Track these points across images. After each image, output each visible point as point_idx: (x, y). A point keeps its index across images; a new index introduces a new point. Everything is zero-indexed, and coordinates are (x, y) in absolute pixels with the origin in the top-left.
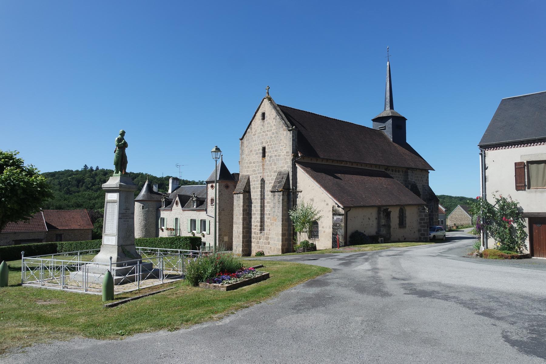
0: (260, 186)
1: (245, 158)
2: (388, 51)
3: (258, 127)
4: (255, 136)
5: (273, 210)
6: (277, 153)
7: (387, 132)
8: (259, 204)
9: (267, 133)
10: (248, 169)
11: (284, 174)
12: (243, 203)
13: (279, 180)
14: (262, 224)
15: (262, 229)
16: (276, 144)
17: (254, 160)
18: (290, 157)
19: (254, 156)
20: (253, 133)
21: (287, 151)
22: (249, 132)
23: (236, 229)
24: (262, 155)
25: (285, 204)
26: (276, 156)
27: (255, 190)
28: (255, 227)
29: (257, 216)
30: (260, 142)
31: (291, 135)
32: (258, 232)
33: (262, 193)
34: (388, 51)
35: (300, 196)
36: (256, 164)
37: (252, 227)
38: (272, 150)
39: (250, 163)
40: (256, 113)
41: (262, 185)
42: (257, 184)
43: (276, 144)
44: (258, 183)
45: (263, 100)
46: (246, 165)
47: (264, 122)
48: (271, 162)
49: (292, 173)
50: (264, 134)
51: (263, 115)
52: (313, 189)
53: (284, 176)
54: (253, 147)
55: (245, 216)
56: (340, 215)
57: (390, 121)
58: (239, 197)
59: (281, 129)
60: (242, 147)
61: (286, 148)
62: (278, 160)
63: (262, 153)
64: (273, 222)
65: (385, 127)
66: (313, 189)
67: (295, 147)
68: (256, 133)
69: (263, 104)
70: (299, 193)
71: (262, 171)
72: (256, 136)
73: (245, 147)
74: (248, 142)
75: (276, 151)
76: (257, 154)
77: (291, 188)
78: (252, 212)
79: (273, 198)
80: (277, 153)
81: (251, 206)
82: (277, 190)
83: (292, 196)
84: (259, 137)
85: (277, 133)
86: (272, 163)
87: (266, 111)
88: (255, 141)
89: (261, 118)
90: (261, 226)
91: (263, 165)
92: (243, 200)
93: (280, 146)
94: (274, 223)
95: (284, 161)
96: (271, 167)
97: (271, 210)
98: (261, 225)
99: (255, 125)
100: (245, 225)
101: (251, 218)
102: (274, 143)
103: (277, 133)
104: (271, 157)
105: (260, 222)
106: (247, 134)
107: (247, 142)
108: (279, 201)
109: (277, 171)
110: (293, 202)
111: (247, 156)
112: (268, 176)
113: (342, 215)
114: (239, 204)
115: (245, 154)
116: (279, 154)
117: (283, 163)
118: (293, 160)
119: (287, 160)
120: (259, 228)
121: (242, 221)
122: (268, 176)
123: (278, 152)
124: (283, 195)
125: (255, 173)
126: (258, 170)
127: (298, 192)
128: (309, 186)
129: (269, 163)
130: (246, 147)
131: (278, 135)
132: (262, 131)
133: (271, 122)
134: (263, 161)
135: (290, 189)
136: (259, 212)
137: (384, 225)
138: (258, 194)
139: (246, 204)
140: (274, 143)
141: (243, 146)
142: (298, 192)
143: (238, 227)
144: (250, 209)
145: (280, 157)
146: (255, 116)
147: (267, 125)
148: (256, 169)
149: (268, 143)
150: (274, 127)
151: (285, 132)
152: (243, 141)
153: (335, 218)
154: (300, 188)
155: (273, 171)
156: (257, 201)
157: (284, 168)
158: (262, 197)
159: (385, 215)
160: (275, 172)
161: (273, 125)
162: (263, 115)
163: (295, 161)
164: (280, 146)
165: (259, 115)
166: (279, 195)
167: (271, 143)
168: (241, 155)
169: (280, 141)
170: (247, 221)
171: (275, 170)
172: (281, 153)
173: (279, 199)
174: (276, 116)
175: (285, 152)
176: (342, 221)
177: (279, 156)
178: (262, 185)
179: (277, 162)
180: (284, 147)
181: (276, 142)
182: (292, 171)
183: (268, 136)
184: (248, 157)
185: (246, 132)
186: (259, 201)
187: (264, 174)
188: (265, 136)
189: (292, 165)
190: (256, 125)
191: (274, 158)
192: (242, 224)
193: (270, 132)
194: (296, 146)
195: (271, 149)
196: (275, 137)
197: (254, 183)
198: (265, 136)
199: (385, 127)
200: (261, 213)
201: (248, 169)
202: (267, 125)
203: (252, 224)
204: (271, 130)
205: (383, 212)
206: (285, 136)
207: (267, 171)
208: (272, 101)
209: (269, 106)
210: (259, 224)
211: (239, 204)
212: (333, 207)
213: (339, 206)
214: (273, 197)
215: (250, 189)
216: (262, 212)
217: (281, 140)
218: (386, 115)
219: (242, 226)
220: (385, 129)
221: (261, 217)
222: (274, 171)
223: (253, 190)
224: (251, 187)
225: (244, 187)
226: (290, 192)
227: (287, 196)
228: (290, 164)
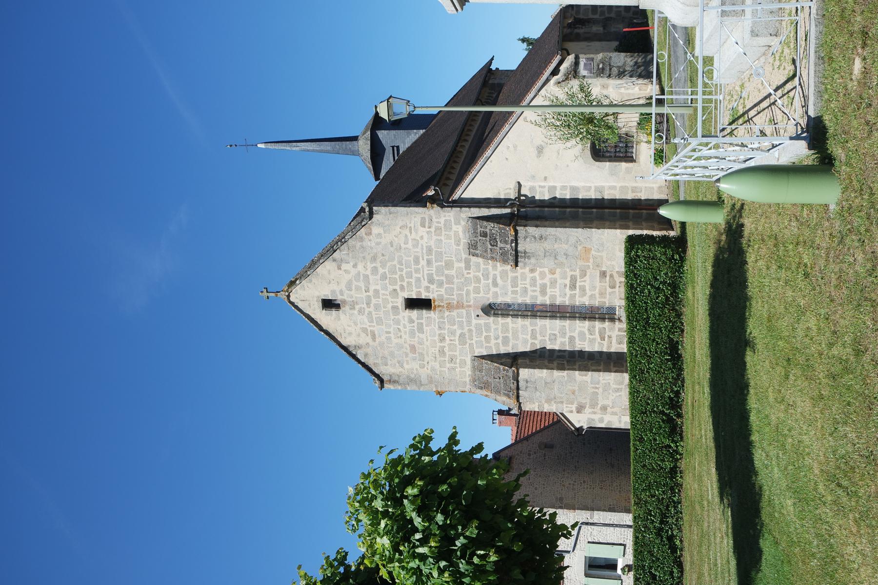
0: (500, 320)
1: (429, 372)
2: (236, 146)
3: (356, 324)
4: (377, 336)
5: (562, 259)
6: (423, 259)
7: (404, 144)
8: (547, 322)
9: (371, 293)
10: (458, 361)
11: (475, 229)
12: (542, 368)
13: (490, 247)
14: (597, 316)
15: (612, 316)
16: (400, 263)
17: (436, 338)
18: (432, 212)
19: (425, 340)
20: (369, 339)
21: (419, 224)
22: (366, 355)
23: (611, 398)
24: (424, 311)
25: (547, 223)
26: (429, 262)
27: (510, 335)
28: (606, 339)
29: (577, 331)
30: (392, 317)
31: (383, 210)
32: (617, 330)
33: (520, 313)
34: (236, 146)
35: (530, 189)
36: (446, 332)
37: (605, 350)
38: (414, 275)
39: (442, 352)
40: (321, 329)
41: (498, 314)
42: (497, 329)
43: (400, 263)
44: (493, 326)
45: (292, 304)
46: (446, 370)
47: (344, 302)
48: (443, 278)
49: (472, 209)
50: (374, 301)
51: (329, 304)
52: (515, 147)
53: (479, 229)
54: (403, 340)
55: (577, 367)
56: (576, 63)
57: (382, 134)
58: (527, 382)
59: (367, 243)
60: (401, 380)
61: (413, 227)
62: (439, 255)
63: (420, 311)
64: (591, 261)
65: (393, 147)
66: (515, 147)
67: (412, 205)
68: (369, 329)
69: (301, 305)
70: (522, 193)
71: (464, 311)
72: (376, 329)
73: (401, 369)
74: (389, 358)
75: (417, 261)
76: (421, 329)
77: (508, 211)
78: (568, 349)
79: (533, 260)
80: (423, 259)
81: (552, 351)
82: (513, 245)
83: (528, 209)
84: (380, 321)
85: (374, 259)
86: (447, 276)
87: (317, 294)
88: (389, 333)
89: (334, 312)
90: (602, 319)
91: (450, 307)
92: (535, 368)
93: (407, 246)
94: (595, 258)
95: (443, 233)
96: (455, 280)
97: (561, 265)
98: (599, 318)
99: (350, 334)
100: (601, 368)
101: (581, 353)
102: (398, 266)
103: (374, 259)
104: (431, 281)
105: (593, 322)
106: (370, 362)
107: (389, 362)
108: (541, 237)
109: (466, 258)
110: (544, 207)
111: (425, 363)
112: (477, 290)
113: (577, 58)
114: (546, 383)
115: (421, 371)
116: (424, 252)
117: (448, 237)
118: (442, 206)
119: (442, 225)
120: (607, 324)
121: (590, 373)
122: (477, 290)
123: (420, 255)
124: (525, 226)
125: (467, 336)
126: (461, 326)
127: (520, 195)
128: (507, 159)
129: (446, 286)
130: (402, 366)
131: (380, 255)
132: (367, 310)
133: (347, 277)
134: (439, 306)
135: (512, 214)
136: (567, 323)
137: (604, 27)
138: (523, 326)
139: (547, 364)
140: (398, 266)
141: (399, 376)
142: (520, 195)
143: (604, 390)
144: (559, 357)
145: (433, 247)
146: (327, 333)
147: (353, 293)
148: (458, 332)
149: (397, 287)
150: (360, 267)
151: (376, 230)
152: (385, 378)
153: (583, 71)
154: (510, 189)
155: (465, 272)
156: (537, 328)
157: (461, 234)
158: (529, 314)
159: (580, 26)
160: (468, 267)
161: (354, 272)
162: (329, 304)
163: (444, 201)
164: (407, 246)
165: (326, 319)
166: (525, 238)
167: (397, 276)
168: (422, 385)
169: (395, 245)
170: (589, 364)
171: (463, 265)
172: (422, 245)
173: (535, 238)
174: (334, 260)
175: (422, 231)
176: (592, 59)
177: (429, 250)
178: (500, 312)
179: (445, 259)
180: (408, 234)
181: (395, 262)
182: (467, 209)
183: (378, 287)
184: (427, 359)
185: (364, 365)
186: (540, 322)
187: (471, 303)
188: (379, 297)
189: (454, 209)
190: (350, 328)
191: (434, 269)
192: (596, 374)
193: (371, 282)
194: (411, 203)
195: (411, 278)
196: (383, 265)
197: (492, 338)
198: (379, 297)
199: (393, 147)
200: (569, 317)
201: (458, 361)
202: (353, 293)
203: (596, 350)
204: (366, 277)
205: (576, 28)
206: (382, 232)
207: (464, 293)
208: (298, 277)
209: (309, 285)
210: (598, 324)
211: (546, 383)
212: (559, 83)
213: (555, 72)
214: (529, 258)
215: (507, 355)
216: (568, 315)
217: (392, 244)
218: (369, 142)
219: (601, 373)
220: (398, 147)
221: (579, 317)
222: (466, 269)
223: (511, 344)
224: (502, 352)
225: (502, 367)
226: (520, 214)
227: (527, 221)
228: (450, 215)
